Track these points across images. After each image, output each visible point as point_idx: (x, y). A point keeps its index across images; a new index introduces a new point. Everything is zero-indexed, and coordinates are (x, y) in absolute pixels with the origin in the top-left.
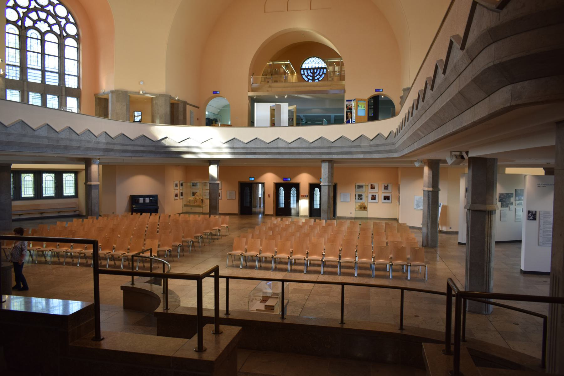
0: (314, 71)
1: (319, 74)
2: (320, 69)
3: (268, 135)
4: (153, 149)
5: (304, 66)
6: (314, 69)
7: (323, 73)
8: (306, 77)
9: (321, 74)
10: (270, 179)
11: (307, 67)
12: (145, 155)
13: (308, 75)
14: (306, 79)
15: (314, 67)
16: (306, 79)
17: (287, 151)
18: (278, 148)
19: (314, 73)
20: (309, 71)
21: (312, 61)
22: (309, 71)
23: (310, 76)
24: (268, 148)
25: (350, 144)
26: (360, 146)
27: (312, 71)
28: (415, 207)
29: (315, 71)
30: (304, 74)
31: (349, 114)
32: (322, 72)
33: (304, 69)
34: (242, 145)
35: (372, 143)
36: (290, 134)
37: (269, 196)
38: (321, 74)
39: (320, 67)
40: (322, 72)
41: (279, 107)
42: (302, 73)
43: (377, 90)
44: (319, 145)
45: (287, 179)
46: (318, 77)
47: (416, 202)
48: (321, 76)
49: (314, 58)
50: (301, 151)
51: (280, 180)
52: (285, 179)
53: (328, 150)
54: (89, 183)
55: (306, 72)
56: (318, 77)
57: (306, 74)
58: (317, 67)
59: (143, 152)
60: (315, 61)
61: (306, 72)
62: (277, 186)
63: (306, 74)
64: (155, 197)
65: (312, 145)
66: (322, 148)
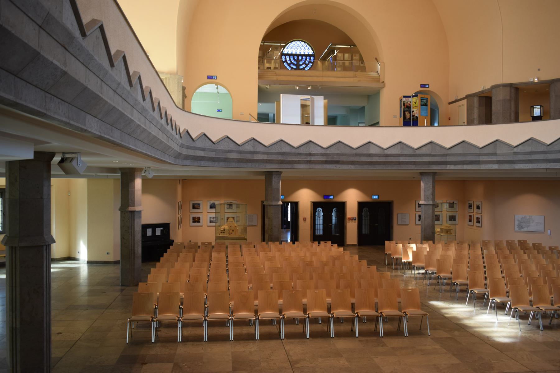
0: (298, 58)
1: (304, 63)
2: (307, 56)
3: (296, 137)
4: (212, 154)
5: (286, 51)
6: (298, 55)
7: (310, 62)
8: (289, 65)
9: (307, 62)
10: (305, 197)
11: (290, 53)
12: (202, 163)
13: (292, 63)
14: (288, 67)
15: (298, 53)
16: (288, 67)
17: (383, 159)
18: (370, 155)
19: (298, 61)
20: (292, 58)
21: (296, 45)
22: (292, 58)
23: (294, 65)
24: (357, 155)
25: (477, 151)
26: (495, 154)
27: (296, 58)
28: (517, 229)
29: (300, 58)
30: (286, 61)
31: (406, 113)
32: (308, 60)
33: (286, 55)
34: (320, 151)
35: (515, 150)
36: (326, 136)
37: (305, 220)
38: (307, 62)
39: (306, 53)
40: (308, 60)
41: (313, 100)
42: (284, 59)
43: (423, 86)
44: (428, 152)
45: (329, 196)
46: (304, 66)
47: (517, 223)
48: (307, 65)
49: (298, 42)
50: (402, 159)
51: (318, 198)
52: (326, 197)
53: (443, 159)
54: (131, 209)
55: (288, 59)
56: (304, 66)
57: (289, 62)
58: (302, 53)
59: (202, 159)
60: (296, 45)
61: (288, 59)
62: (315, 205)
63: (289, 62)
64: (166, 227)
65: (417, 152)
66: (434, 155)
